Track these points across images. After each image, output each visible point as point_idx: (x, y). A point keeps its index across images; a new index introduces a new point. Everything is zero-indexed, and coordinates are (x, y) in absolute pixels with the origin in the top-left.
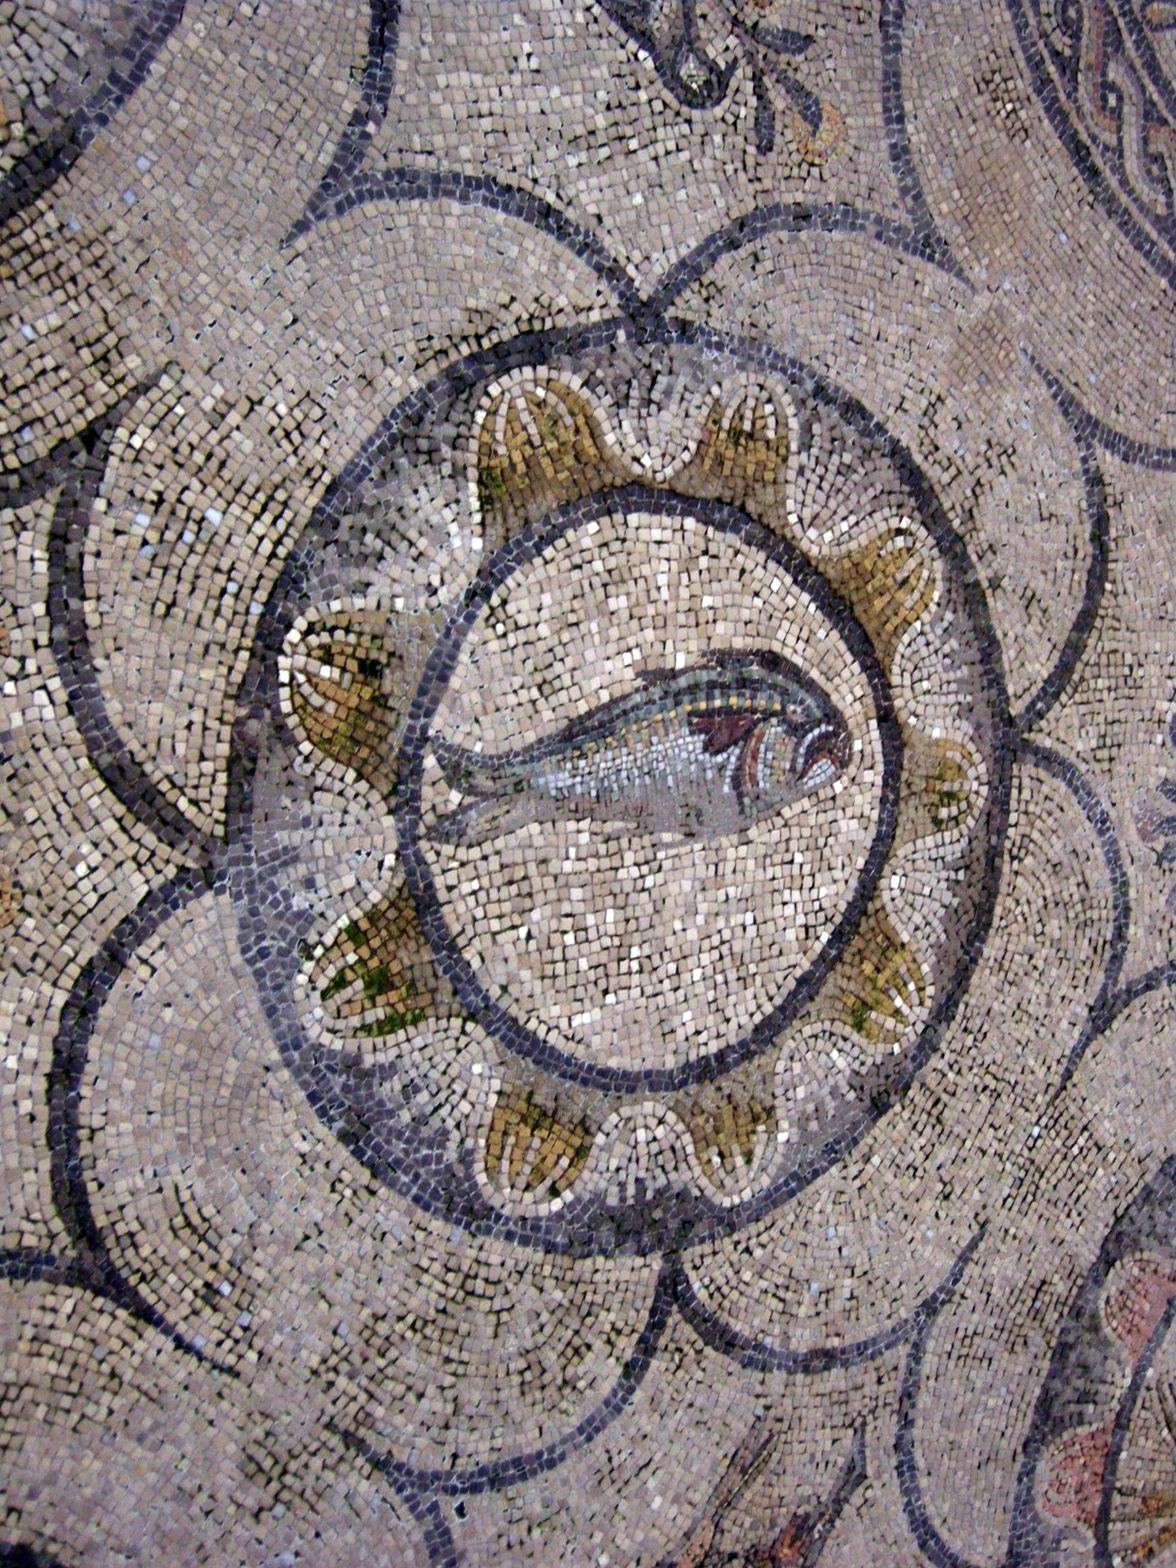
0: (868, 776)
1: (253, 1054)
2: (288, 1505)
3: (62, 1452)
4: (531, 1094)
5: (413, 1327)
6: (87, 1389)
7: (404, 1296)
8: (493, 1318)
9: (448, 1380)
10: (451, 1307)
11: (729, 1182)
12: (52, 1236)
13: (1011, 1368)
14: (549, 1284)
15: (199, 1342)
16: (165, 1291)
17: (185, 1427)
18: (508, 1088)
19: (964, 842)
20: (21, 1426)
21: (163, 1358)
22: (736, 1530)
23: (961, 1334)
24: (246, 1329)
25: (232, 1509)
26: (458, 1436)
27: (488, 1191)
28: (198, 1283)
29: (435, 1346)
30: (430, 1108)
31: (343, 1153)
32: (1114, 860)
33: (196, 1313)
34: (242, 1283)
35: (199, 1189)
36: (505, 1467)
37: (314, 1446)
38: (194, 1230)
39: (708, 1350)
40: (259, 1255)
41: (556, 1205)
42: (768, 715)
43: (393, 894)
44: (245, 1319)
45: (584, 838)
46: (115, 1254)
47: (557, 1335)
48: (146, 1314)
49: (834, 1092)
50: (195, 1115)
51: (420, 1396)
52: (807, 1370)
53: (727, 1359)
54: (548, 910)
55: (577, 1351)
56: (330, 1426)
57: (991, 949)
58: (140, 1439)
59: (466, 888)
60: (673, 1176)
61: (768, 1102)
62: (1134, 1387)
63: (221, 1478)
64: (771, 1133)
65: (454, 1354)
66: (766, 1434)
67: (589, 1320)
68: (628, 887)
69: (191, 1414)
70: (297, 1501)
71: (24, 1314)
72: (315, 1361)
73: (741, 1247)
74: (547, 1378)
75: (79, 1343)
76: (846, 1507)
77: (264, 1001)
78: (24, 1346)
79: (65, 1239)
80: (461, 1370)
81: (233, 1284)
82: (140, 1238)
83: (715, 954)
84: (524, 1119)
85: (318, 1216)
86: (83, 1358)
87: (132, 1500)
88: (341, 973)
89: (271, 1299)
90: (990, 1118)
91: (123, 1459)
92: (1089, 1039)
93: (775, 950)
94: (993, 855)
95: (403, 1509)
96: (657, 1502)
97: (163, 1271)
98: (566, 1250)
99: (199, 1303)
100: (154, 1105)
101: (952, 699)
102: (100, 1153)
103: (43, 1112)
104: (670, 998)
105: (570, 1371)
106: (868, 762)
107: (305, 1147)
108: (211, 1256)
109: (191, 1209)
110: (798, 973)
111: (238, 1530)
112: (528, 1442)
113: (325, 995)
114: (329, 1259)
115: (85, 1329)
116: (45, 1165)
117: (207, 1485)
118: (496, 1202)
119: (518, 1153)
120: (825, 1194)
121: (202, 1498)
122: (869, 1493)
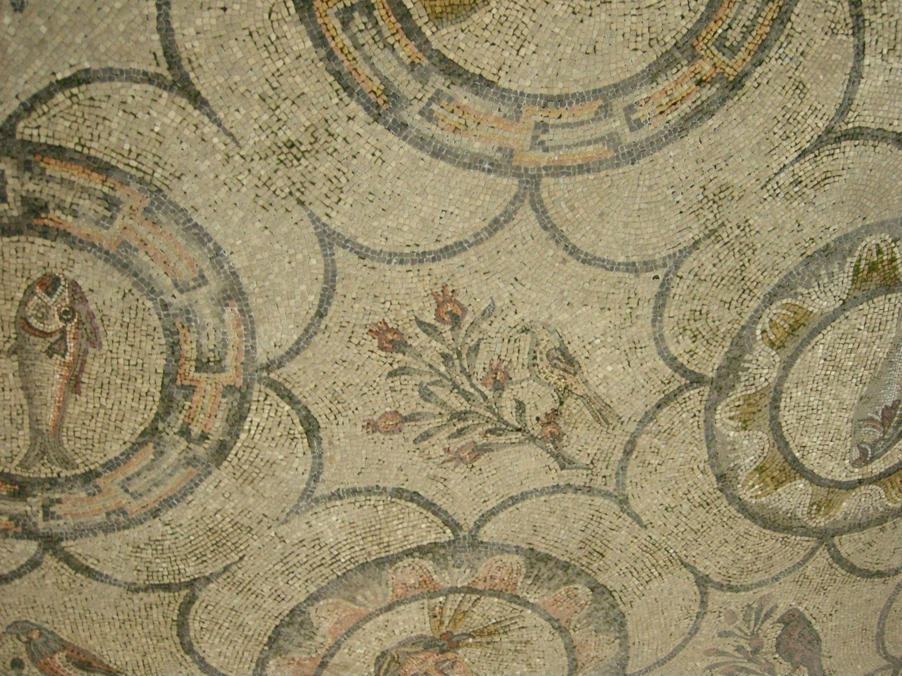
0: (844, 475)
1: (872, 214)
2: (701, 202)
3: (770, 110)
4: (804, 325)
5: (744, 265)
6: (788, 125)
7: (757, 263)
8: (729, 300)
9: (714, 278)
10: (743, 282)
11: (728, 408)
12: (847, 123)
13: (574, 541)
14: (729, 326)
15: (782, 175)
16: (807, 164)
17: (753, 163)
18: (812, 316)
19: (800, 516)
20: (788, 96)
21: (784, 158)
22: (574, 405)
23: (604, 516)
24: (777, 195)
25: (712, 177)
26: (689, 280)
27: (779, 303)
28: (803, 178)
29: (731, 274)
30: (821, 282)
31: (821, 244)
32: (760, 584)
33: (794, 175)
34: (796, 196)
35: (837, 185)
36: (665, 300)
37: (718, 216)
38: (823, 180)
39: (663, 395)
40: (803, 204)
41: (758, 332)
42: (884, 433)
43: (898, 277)
44: (781, 195)
45: (881, 355)
46: (829, 147)
47: (706, 326)
48: (803, 154)
49: (738, 457)
50: (862, 188)
51: (714, 265)
52: (629, 442)
53: (653, 404)
54: (864, 338)
55: (695, 336)
56: (723, 224)
57: (755, 529)
58: (758, 143)
59: (887, 305)
60: (743, 384)
61: (749, 428)
62: (526, 604)
63: (727, 174)
64: (736, 429)
65: (724, 282)
66: (610, 421)
67: (705, 342)
68: (857, 371)
69: (757, 166)
70: (700, 205)
71: (826, 107)
72: (751, 222)
73: (697, 413)
74: (692, 322)
75: (806, 126)
76: (552, 459)
77: (887, 221)
78: (815, 104)
79: (844, 128)
80: (716, 284)
81: (796, 192)
82: (830, 158)
83: (815, 407)
84: (796, 321)
85: (804, 231)
86: (799, 126)
87: (737, 136)
88: (882, 253)
89: (783, 207)
90: (689, 529)
91: (755, 134)
92: (695, 575)
93: (804, 433)
94: (788, 529)
95: (671, 252)
96: (610, 368)
97: (814, 165)
98: (739, 336)
99: (796, 177)
100: (873, 171)
101: (853, 511)
102: (867, 148)
103: (890, 129)
104: (809, 387)
105: (688, 332)
106: (850, 474)
107: (831, 229)
108: (811, 185)
109: (831, 180)
110: (791, 443)
111: (702, 178)
112: (671, 310)
113: (878, 245)
114: (786, 233)
115: (810, 129)
116: (873, 126)
117: (727, 168)
118: (773, 307)
119: (786, 317)
120: (698, 452)
121: (723, 165)
122: (554, 471)
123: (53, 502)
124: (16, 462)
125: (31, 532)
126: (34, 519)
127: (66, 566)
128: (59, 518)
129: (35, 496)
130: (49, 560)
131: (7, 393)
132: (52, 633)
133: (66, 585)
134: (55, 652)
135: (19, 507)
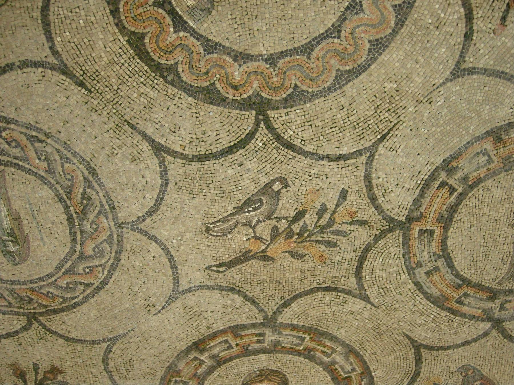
123: (507, 302)
124: (497, 281)
125: (490, 318)
126: (494, 311)
127: (500, 335)
128: (507, 310)
129: (499, 299)
130: (494, 332)
131: (505, 246)
132: (479, 371)
133: (497, 345)
134: (476, 381)
135: (490, 305)
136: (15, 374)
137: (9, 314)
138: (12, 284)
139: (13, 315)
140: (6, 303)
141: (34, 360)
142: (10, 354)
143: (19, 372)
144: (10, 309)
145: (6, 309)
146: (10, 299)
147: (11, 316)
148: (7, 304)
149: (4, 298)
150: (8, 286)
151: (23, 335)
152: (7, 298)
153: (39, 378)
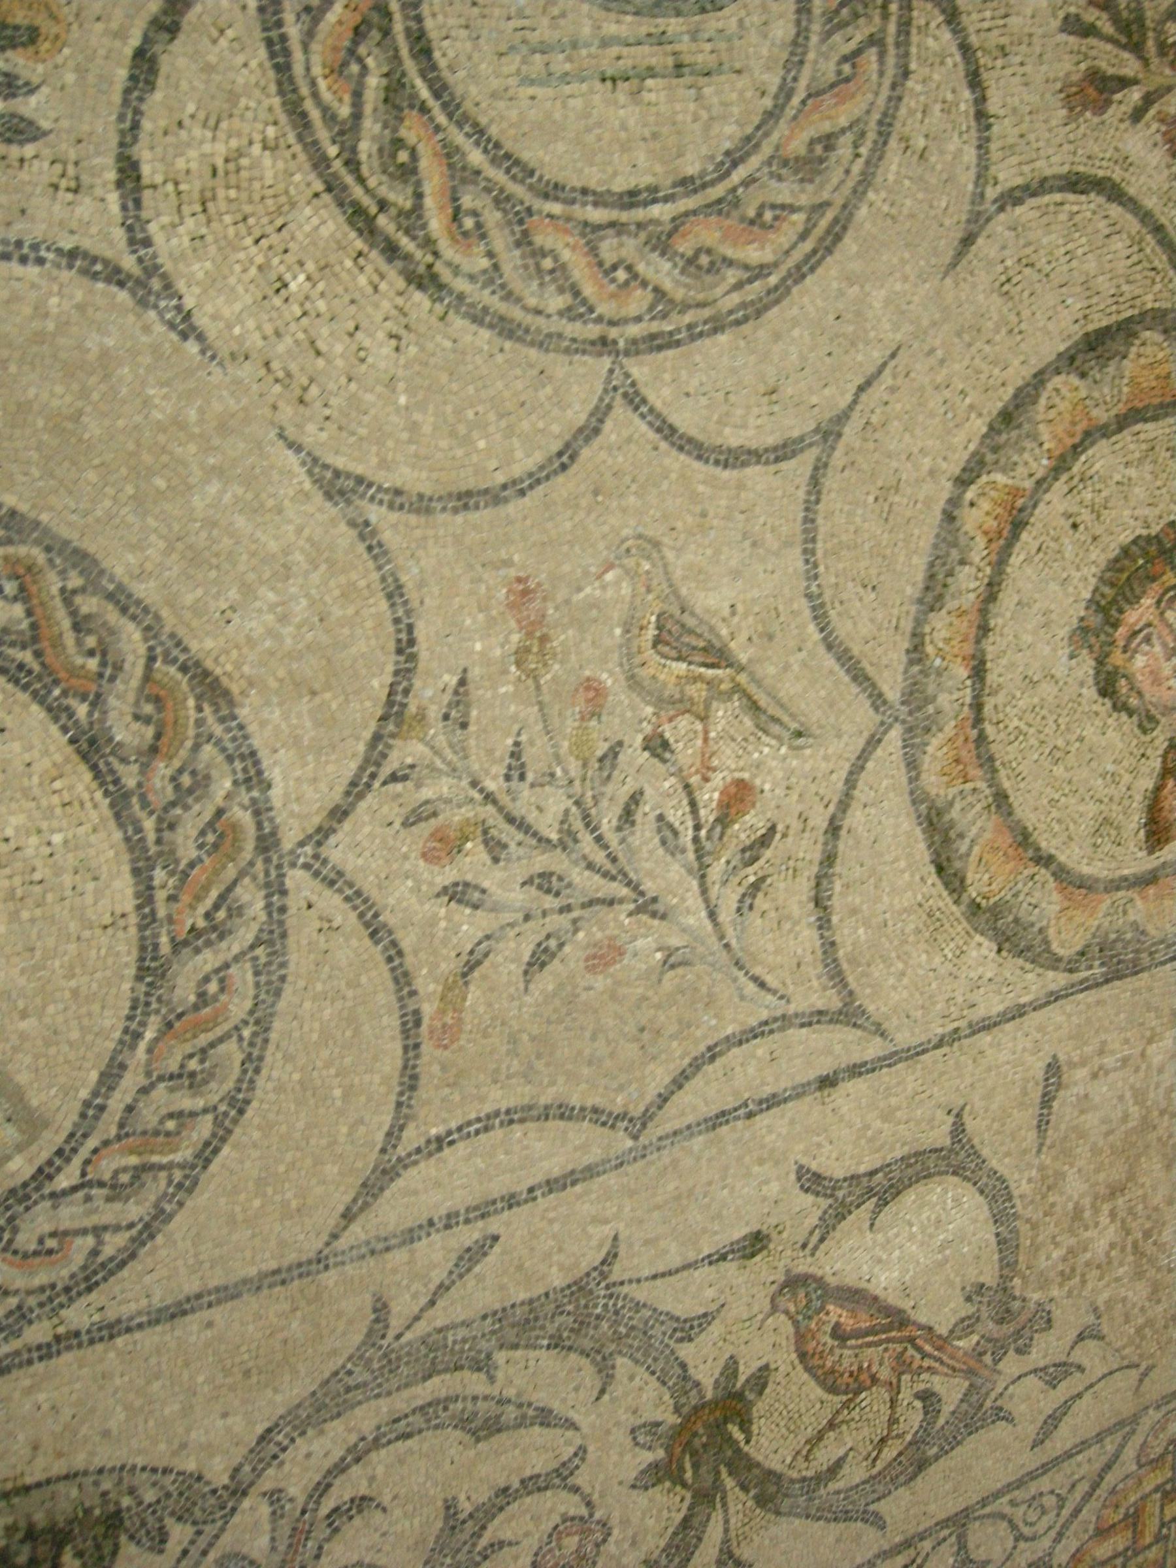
136: (1101, 107)
137: (907, 54)
138: (809, 11)
139: (908, 43)
140: (872, 54)
141: (1056, 24)
142: (1034, 99)
143: (1091, 92)
144: (892, 51)
145: (891, 60)
146: (859, 37)
147: (914, 50)
148: (874, 50)
149: (857, 53)
150: (816, 27)
151: (971, 29)
152: (853, 45)
153: (1108, 28)
